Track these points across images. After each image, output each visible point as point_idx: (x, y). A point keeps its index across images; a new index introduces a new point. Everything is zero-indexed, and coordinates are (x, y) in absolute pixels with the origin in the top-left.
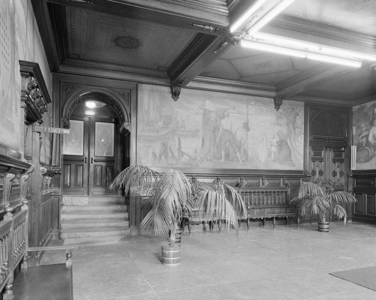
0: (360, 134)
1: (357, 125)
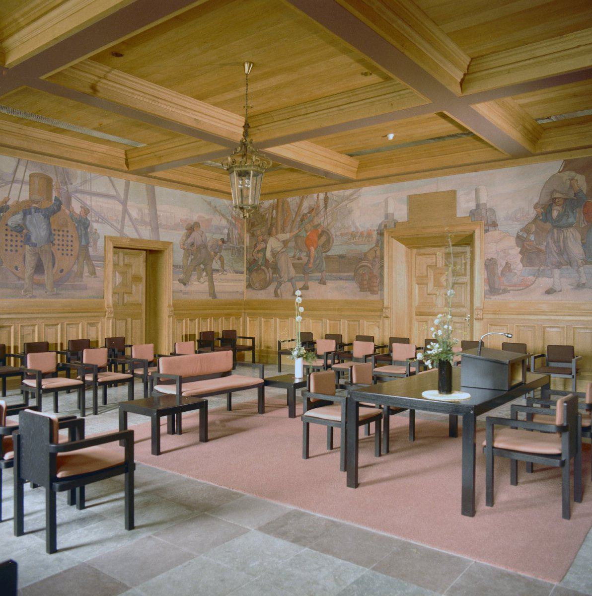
0: (256, 246)
1: (252, 232)
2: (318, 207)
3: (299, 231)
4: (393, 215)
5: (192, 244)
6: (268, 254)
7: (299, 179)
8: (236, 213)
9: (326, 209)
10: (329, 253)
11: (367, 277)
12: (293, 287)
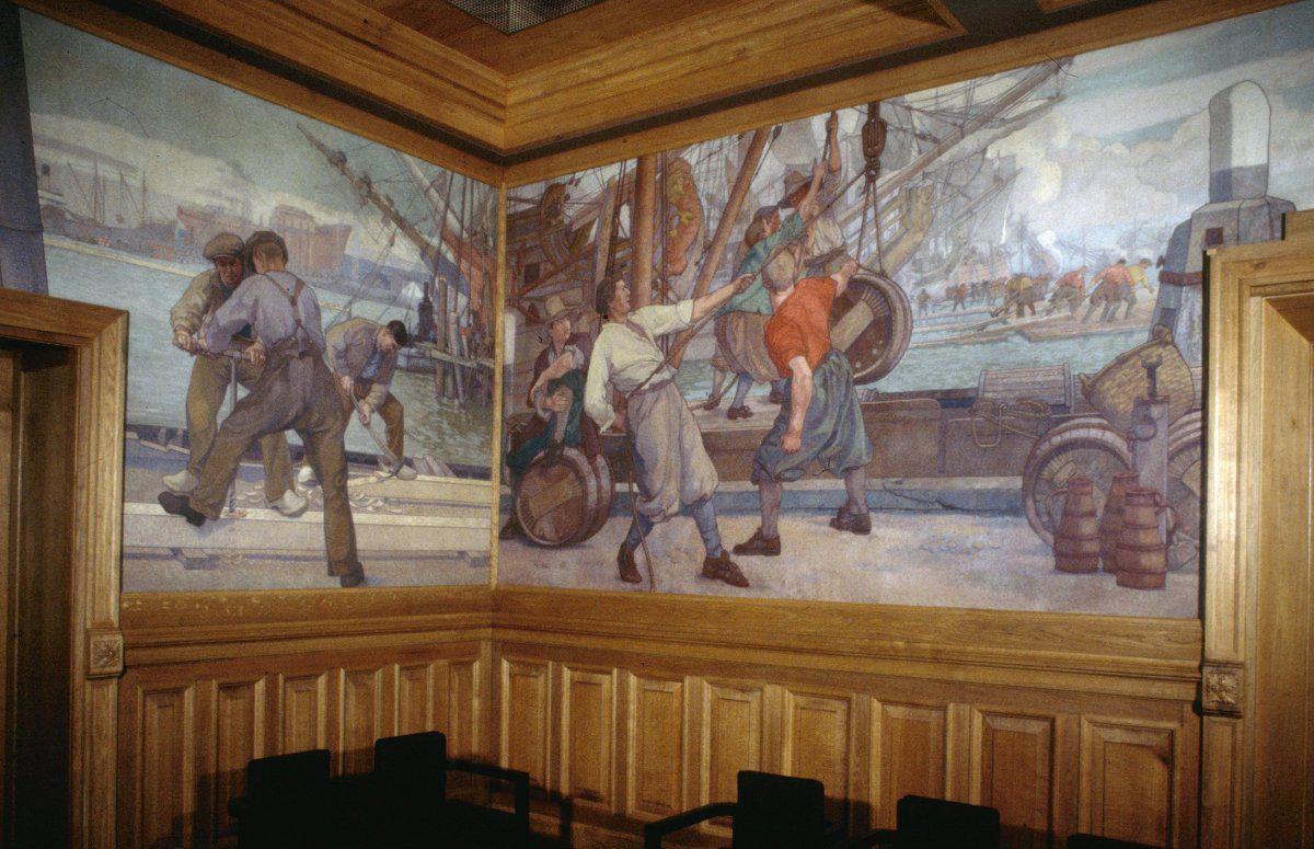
0: (542, 363)
1: (526, 305)
2: (832, 171)
3: (739, 291)
4: (1263, 173)
5: (243, 334)
6: (595, 397)
7: (750, 43)
8: (461, 222)
9: (871, 180)
10: (886, 385)
11: (1097, 499)
12: (706, 541)
